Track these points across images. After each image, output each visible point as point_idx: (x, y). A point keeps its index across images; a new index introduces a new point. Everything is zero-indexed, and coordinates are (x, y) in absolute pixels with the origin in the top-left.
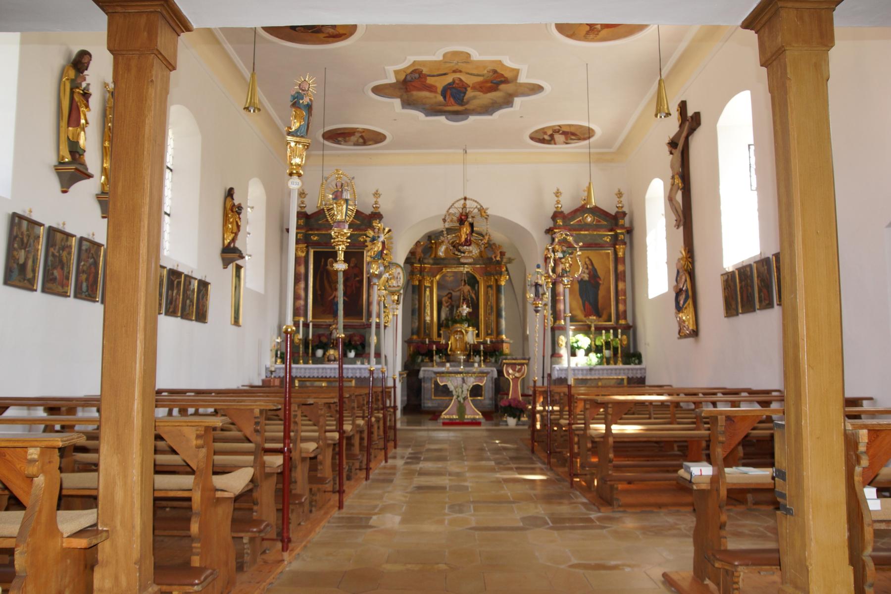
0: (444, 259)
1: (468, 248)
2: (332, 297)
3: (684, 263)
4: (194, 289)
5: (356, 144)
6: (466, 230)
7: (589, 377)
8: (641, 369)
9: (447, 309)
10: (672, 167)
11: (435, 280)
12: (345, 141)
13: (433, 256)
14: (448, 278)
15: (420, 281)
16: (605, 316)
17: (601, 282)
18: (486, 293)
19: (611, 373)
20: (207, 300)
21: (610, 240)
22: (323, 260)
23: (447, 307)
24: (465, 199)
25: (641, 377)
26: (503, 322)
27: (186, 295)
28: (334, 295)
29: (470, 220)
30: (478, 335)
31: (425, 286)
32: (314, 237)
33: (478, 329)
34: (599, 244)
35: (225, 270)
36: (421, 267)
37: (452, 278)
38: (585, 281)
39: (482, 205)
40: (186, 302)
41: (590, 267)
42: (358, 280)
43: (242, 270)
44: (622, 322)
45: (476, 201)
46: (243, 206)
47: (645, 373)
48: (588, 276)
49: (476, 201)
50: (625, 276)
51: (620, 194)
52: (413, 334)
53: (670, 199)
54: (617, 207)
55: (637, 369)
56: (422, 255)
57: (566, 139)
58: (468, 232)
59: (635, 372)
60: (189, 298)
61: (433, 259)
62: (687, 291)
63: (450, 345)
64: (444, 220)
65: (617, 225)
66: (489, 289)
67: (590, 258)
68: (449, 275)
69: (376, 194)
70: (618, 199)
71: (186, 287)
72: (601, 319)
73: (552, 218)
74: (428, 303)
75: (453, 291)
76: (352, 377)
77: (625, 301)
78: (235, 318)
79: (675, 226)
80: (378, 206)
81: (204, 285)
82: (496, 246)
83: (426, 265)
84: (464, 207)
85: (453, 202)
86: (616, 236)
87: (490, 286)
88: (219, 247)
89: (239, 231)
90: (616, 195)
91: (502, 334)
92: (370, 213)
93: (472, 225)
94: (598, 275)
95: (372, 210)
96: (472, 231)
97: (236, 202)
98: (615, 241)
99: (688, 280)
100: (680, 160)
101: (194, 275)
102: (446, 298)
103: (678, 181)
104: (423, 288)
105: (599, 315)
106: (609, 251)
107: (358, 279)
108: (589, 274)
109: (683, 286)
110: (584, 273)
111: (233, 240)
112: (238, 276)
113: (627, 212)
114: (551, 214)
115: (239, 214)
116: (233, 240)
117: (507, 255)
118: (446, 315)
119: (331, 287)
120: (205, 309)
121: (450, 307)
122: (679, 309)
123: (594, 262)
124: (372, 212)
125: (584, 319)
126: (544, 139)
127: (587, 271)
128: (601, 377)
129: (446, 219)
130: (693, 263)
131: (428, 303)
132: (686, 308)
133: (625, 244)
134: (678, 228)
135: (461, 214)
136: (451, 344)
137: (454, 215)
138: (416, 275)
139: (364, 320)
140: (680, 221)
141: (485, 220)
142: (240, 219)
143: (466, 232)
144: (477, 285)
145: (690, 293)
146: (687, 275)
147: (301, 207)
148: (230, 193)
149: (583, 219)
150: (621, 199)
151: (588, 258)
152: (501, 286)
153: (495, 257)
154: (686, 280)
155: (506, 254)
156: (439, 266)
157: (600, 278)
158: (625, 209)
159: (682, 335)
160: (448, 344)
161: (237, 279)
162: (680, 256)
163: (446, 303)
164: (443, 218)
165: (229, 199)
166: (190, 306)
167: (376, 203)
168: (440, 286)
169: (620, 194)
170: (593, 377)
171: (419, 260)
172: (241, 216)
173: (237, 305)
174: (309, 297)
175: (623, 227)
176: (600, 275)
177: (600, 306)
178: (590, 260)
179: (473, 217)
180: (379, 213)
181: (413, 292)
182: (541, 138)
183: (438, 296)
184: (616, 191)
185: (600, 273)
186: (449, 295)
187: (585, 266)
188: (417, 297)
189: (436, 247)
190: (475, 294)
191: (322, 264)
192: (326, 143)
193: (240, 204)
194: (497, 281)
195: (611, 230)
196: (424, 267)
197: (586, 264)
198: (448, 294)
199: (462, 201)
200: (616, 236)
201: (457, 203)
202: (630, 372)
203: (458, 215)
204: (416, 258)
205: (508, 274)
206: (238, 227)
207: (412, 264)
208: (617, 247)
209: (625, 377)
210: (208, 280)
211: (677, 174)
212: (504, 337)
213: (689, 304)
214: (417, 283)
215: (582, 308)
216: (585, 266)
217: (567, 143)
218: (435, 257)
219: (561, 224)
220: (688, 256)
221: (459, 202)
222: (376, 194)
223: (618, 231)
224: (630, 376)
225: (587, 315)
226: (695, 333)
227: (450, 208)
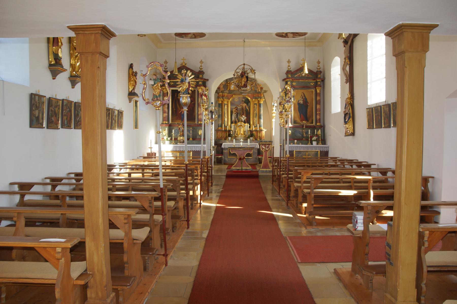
0: (233, 91)
1: (245, 88)
2: (180, 112)
3: (349, 101)
4: (116, 115)
5: (191, 38)
6: (244, 80)
7: (302, 151)
8: (326, 147)
9: (235, 115)
10: (345, 52)
11: (229, 101)
12: (186, 37)
13: (228, 89)
14: (235, 100)
15: (222, 101)
16: (310, 121)
17: (309, 105)
18: (254, 107)
19: (313, 149)
20: (122, 119)
21: (314, 84)
22: (176, 94)
23: (235, 113)
24: (244, 64)
25: (326, 151)
26: (262, 121)
27: (112, 118)
28: (181, 111)
29: (246, 75)
30: (250, 127)
31: (225, 104)
32: (171, 83)
33: (250, 124)
34: (308, 86)
35: (130, 103)
36: (223, 95)
37: (237, 100)
38: (302, 104)
39: (252, 67)
40: (113, 121)
41: (304, 97)
42: (193, 104)
43: (138, 103)
44: (318, 124)
45: (249, 66)
46: (137, 72)
47: (328, 149)
48: (303, 101)
49: (249, 66)
50: (320, 102)
51: (319, 62)
52: (219, 127)
53: (343, 69)
54: (317, 69)
55: (325, 147)
56: (223, 89)
57: (294, 35)
58: (245, 81)
59: (324, 148)
60: (114, 119)
61: (228, 91)
62: (350, 114)
63: (236, 132)
64: (234, 75)
65: (317, 77)
66: (255, 105)
67: (304, 93)
68: (236, 98)
69: (201, 62)
70: (318, 65)
71: (112, 114)
72: (308, 122)
73: (286, 73)
74: (226, 112)
75: (238, 106)
76: (191, 151)
77: (320, 114)
78: (135, 126)
79: (345, 83)
80: (202, 68)
81: (120, 113)
82: (259, 85)
83: (225, 94)
84: (244, 68)
85: (238, 66)
86: (316, 83)
87: (256, 104)
88: (127, 93)
89: (136, 84)
90: (317, 62)
91: (261, 127)
92: (198, 71)
93: (247, 77)
94: (307, 101)
95: (199, 70)
96: (247, 80)
97: (134, 71)
98: (316, 85)
99: (351, 109)
100: (349, 50)
101: (116, 108)
102: (235, 109)
103: (347, 60)
104: (224, 104)
105: (307, 120)
106: (313, 90)
107: (193, 103)
108: (303, 101)
109: (348, 112)
110: (301, 100)
111: (134, 89)
112: (136, 106)
113: (322, 71)
114: (286, 72)
115: (136, 76)
116: (134, 89)
117: (264, 89)
118: (235, 118)
119: (180, 107)
120: (121, 124)
121: (236, 114)
122: (346, 123)
123: (306, 95)
124: (199, 71)
125: (301, 122)
126: (282, 35)
127: (302, 99)
128: (308, 151)
129: (235, 74)
130: (353, 101)
131: (226, 112)
132: (349, 122)
133: (321, 86)
134: (346, 83)
135: (242, 72)
136: (237, 131)
137: (239, 72)
138: (220, 98)
139: (196, 122)
140: (348, 80)
141: (254, 75)
142: (136, 78)
143: (244, 81)
144: (249, 103)
145: (351, 115)
146: (350, 106)
147: (165, 69)
148: (131, 66)
149: (301, 74)
150: (319, 65)
151: (303, 93)
152: (261, 104)
153: (258, 90)
154: (349, 109)
155: (263, 88)
156: (231, 94)
157: (308, 102)
158: (321, 70)
159: (347, 135)
160: (236, 131)
161: (136, 107)
162: (347, 97)
163: (235, 112)
164: (234, 74)
165: (131, 69)
166: (114, 123)
167: (201, 66)
168: (232, 104)
169: (319, 62)
170: (304, 150)
171: (222, 92)
172: (137, 77)
173: (136, 123)
174: (170, 112)
175: (320, 78)
176: (308, 102)
177: (308, 116)
178: (304, 94)
179: (248, 74)
180: (203, 71)
181: (219, 107)
182: (281, 35)
183: (231, 108)
184: (317, 61)
185: (309, 100)
186: (236, 108)
187: (301, 97)
188: (221, 109)
189: (230, 85)
190: (249, 108)
191: (176, 96)
192: (177, 38)
193: (136, 71)
194: (259, 101)
195: (314, 80)
196: (224, 95)
197: (302, 95)
198: (236, 107)
199: (243, 66)
200: (316, 83)
201: (240, 67)
202: (322, 148)
203: (240, 72)
204: (220, 90)
205: (264, 98)
206: (136, 82)
207: (218, 93)
208: (317, 88)
209: (319, 151)
210: (122, 110)
211: (347, 57)
212: (262, 128)
213: (350, 120)
214: (221, 103)
215: (300, 117)
216: (301, 97)
217: (294, 37)
218: (229, 90)
219: (290, 76)
220: (351, 98)
221: (241, 66)
222: (201, 62)
223: (318, 80)
224: (322, 150)
225: (302, 120)
226: (353, 134)
227: (237, 69)
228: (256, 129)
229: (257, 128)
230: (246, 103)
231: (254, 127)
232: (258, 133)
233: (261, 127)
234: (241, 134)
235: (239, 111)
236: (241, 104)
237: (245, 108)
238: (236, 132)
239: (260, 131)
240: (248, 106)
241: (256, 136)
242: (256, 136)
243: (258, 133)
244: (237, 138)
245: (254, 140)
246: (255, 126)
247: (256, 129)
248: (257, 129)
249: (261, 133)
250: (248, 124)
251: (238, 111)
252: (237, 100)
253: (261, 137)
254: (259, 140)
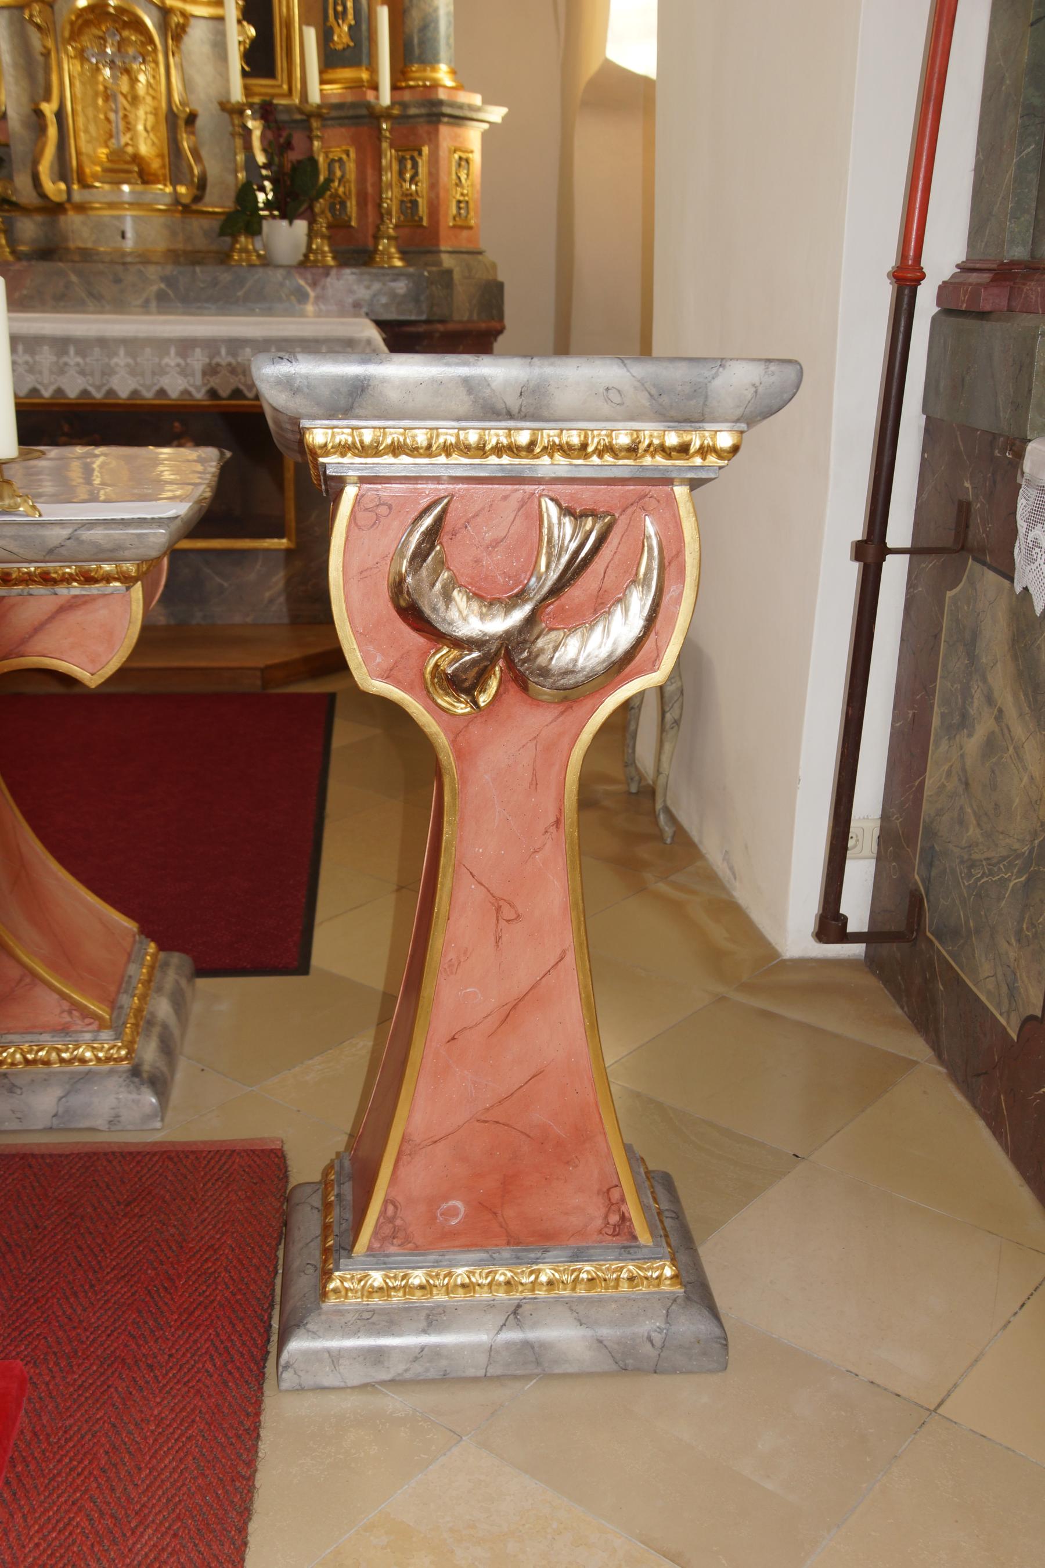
63: (52, 131)
212: (443, 74)
228: (356, 86)
229: (365, 75)
231: (330, 59)
232: (389, 155)
233: (429, 60)
234: (136, 158)
238: (52, 131)
239: (423, 129)
241: (362, 203)
242: (352, 206)
243: (379, 155)
244: (72, 220)
245: (329, 260)
246: (342, 35)
247: (350, 98)
248: (370, 95)
249: (434, 160)
253: (423, 209)
254: (398, 263)
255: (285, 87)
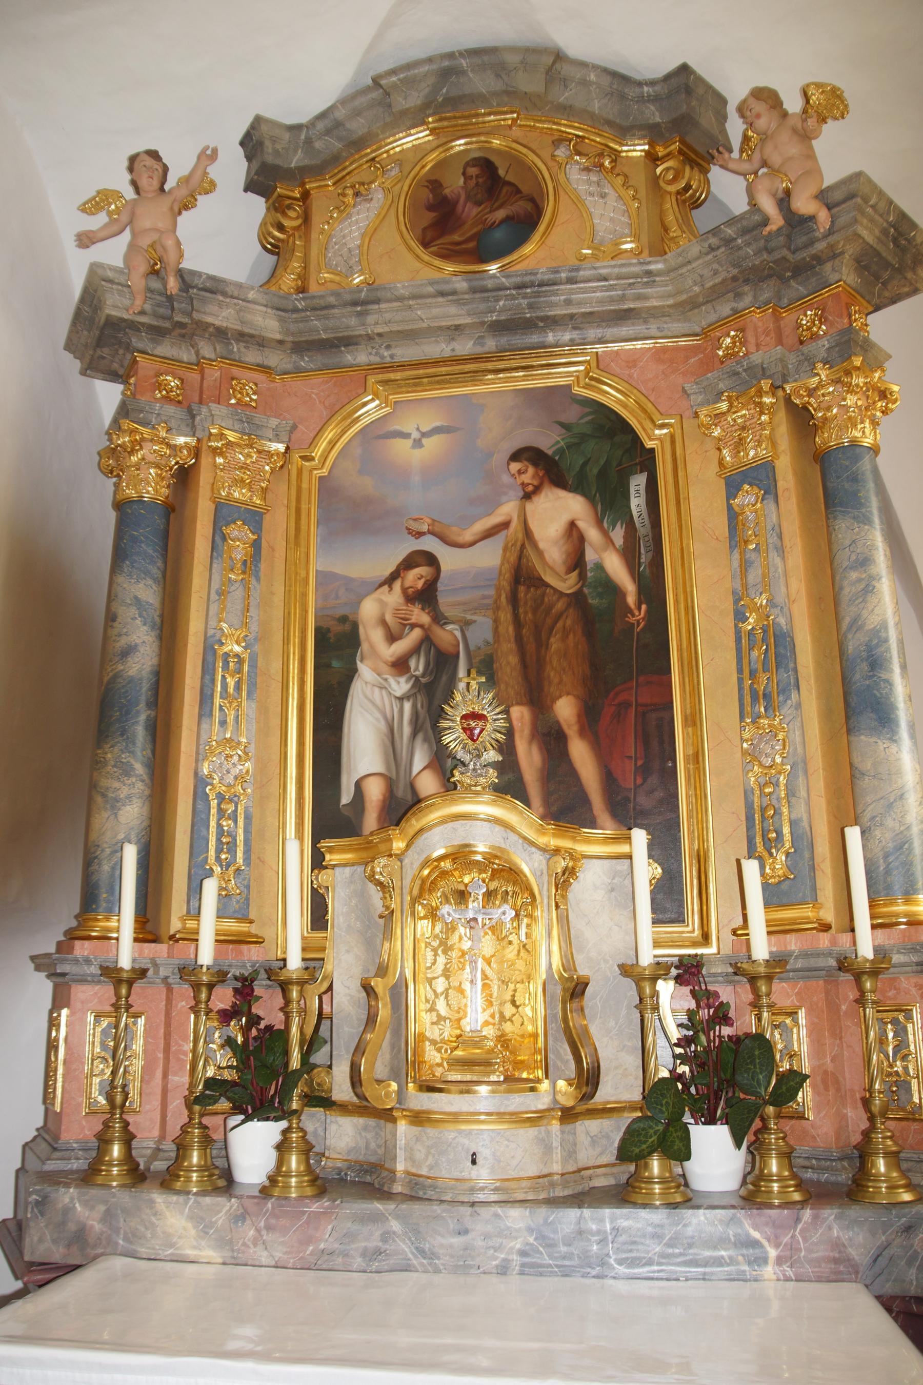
9: (401, 686)
23: (400, 665)
37: (432, 444)
61: (282, 309)
66: (747, 498)
102: (394, 597)
121: (418, 666)
144: (638, 482)
163: (392, 638)
186: (416, 577)
190: (629, 554)
198: (409, 563)
218: (302, 290)
230: (578, 487)
235: (465, 624)
236: (494, 504)
237: (577, 562)
240: (618, 535)
250: (640, 837)
251: (439, 619)
252: (432, 444)
255: (697, 933)
